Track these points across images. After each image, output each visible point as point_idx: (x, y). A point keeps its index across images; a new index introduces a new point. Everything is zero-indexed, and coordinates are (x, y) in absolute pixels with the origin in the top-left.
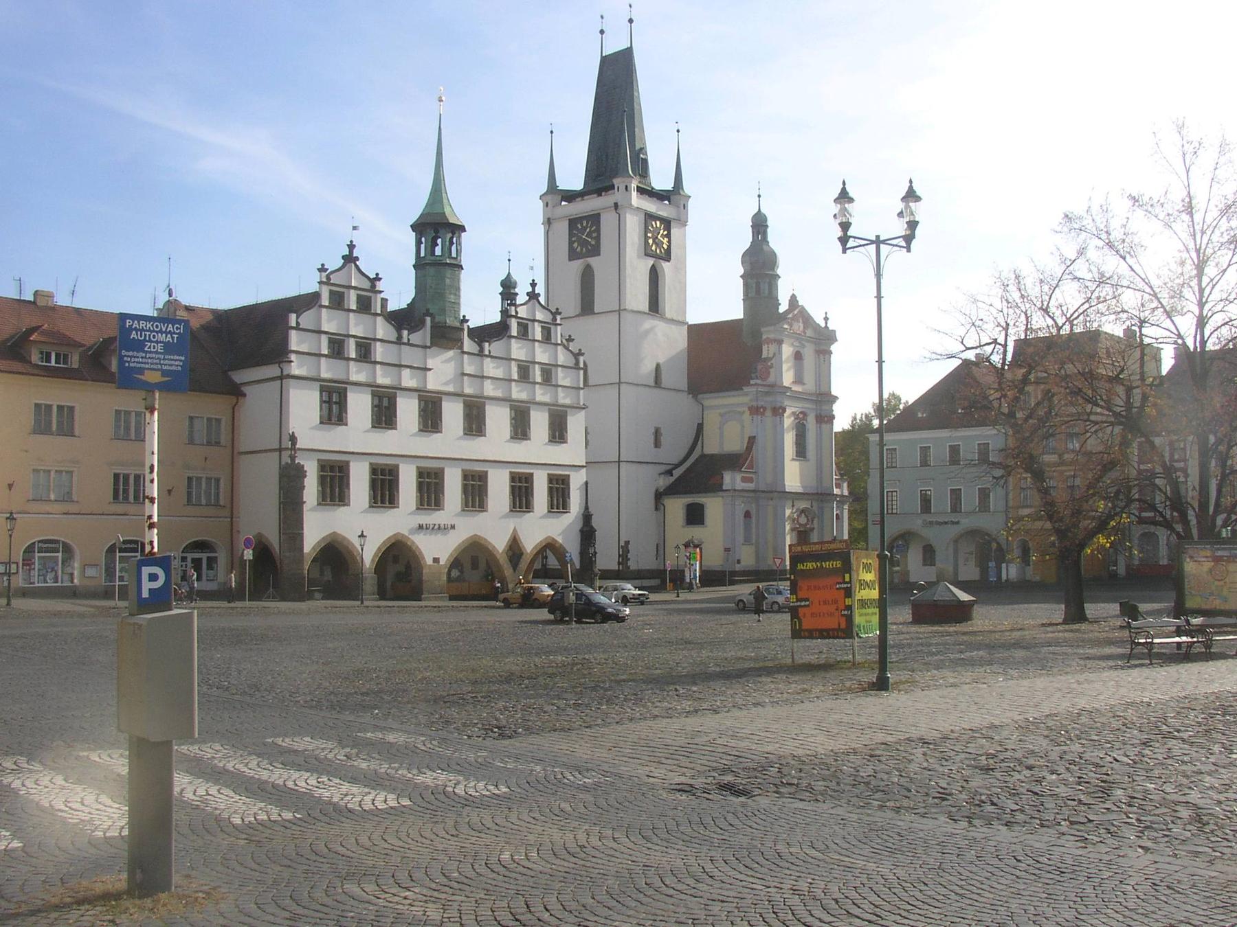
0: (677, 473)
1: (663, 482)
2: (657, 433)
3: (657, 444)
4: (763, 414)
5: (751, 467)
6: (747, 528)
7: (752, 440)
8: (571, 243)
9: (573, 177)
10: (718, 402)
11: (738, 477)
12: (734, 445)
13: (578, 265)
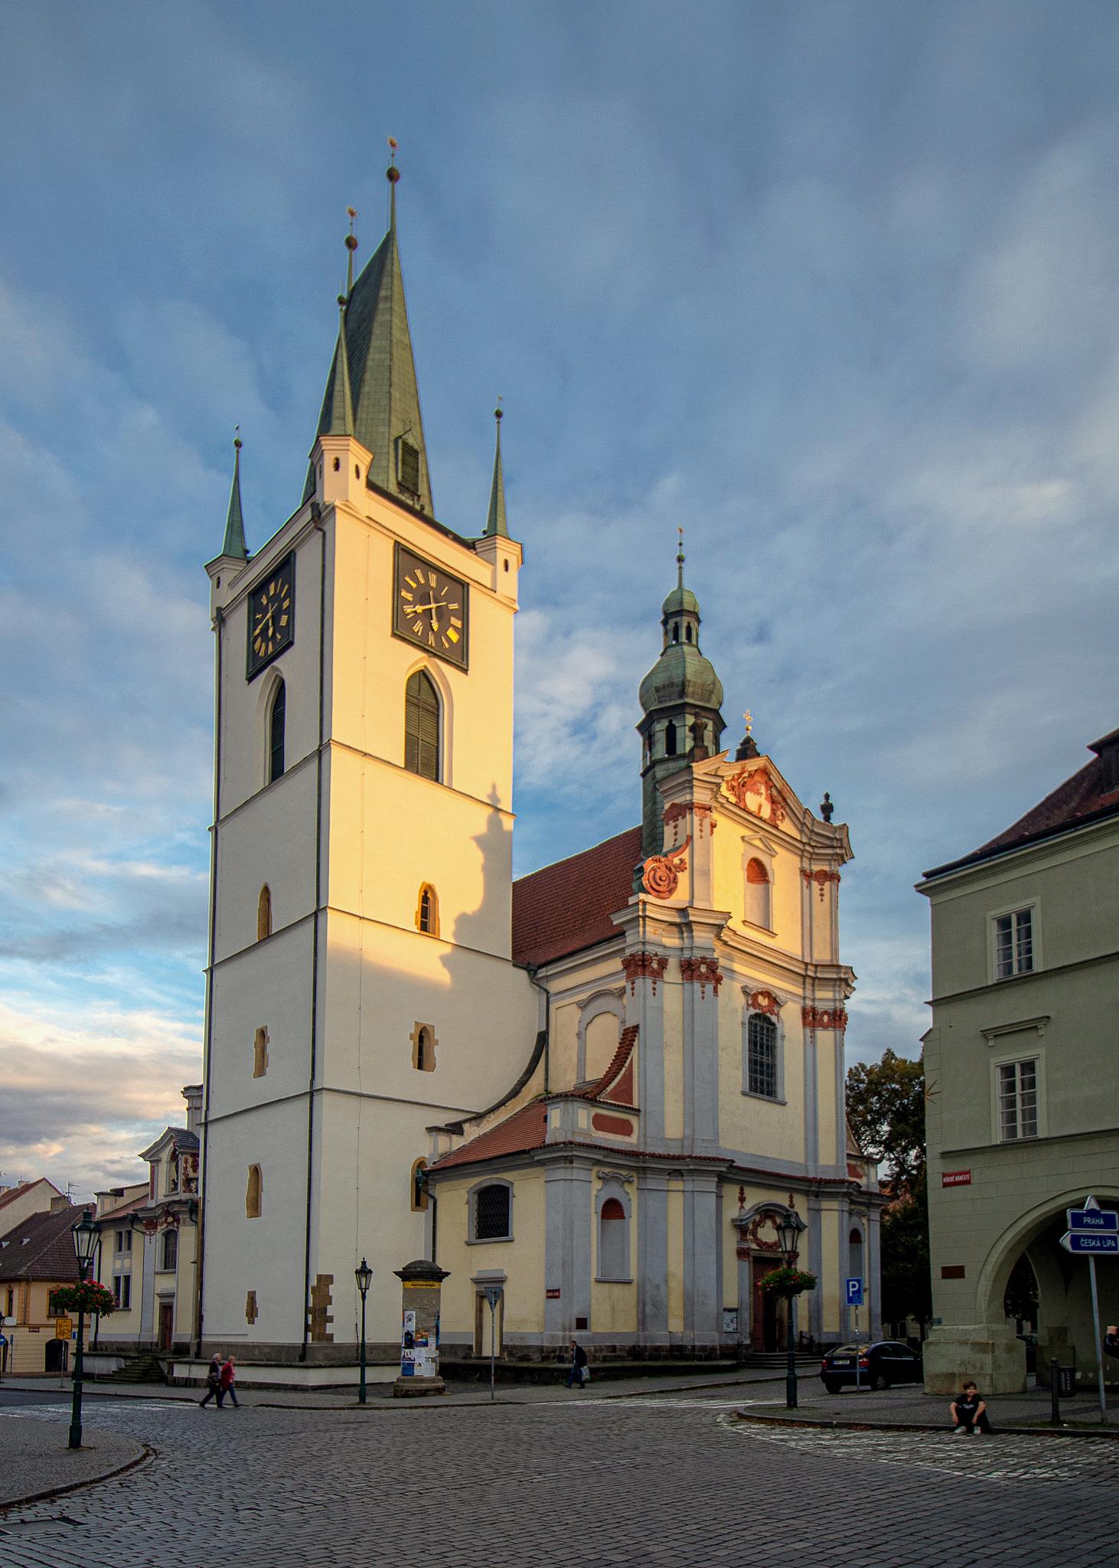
0: (472, 1132)
1: (433, 1149)
2: (423, 1039)
4: (658, 975)
5: (625, 1091)
7: (629, 1036)
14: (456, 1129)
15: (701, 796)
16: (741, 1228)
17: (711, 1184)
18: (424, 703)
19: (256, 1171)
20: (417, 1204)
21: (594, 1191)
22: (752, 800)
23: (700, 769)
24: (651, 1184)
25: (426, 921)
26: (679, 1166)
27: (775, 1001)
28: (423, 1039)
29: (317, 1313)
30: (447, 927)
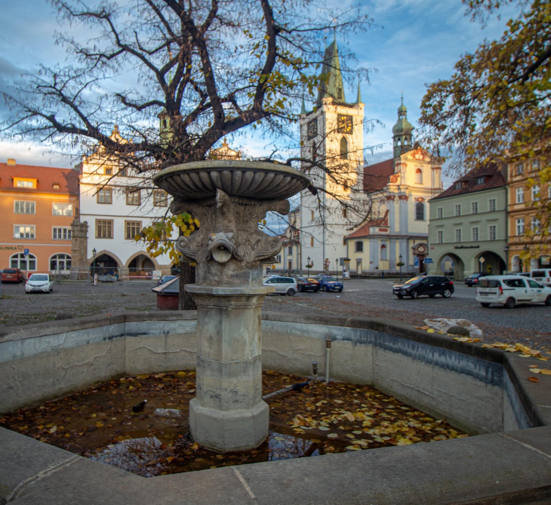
0: (355, 229)
1: (347, 233)
4: (393, 200)
14: (352, 229)
15: (402, 161)
16: (414, 249)
17: (405, 241)
21: (380, 243)
22: (417, 156)
23: (402, 156)
24: (392, 241)
26: (397, 237)
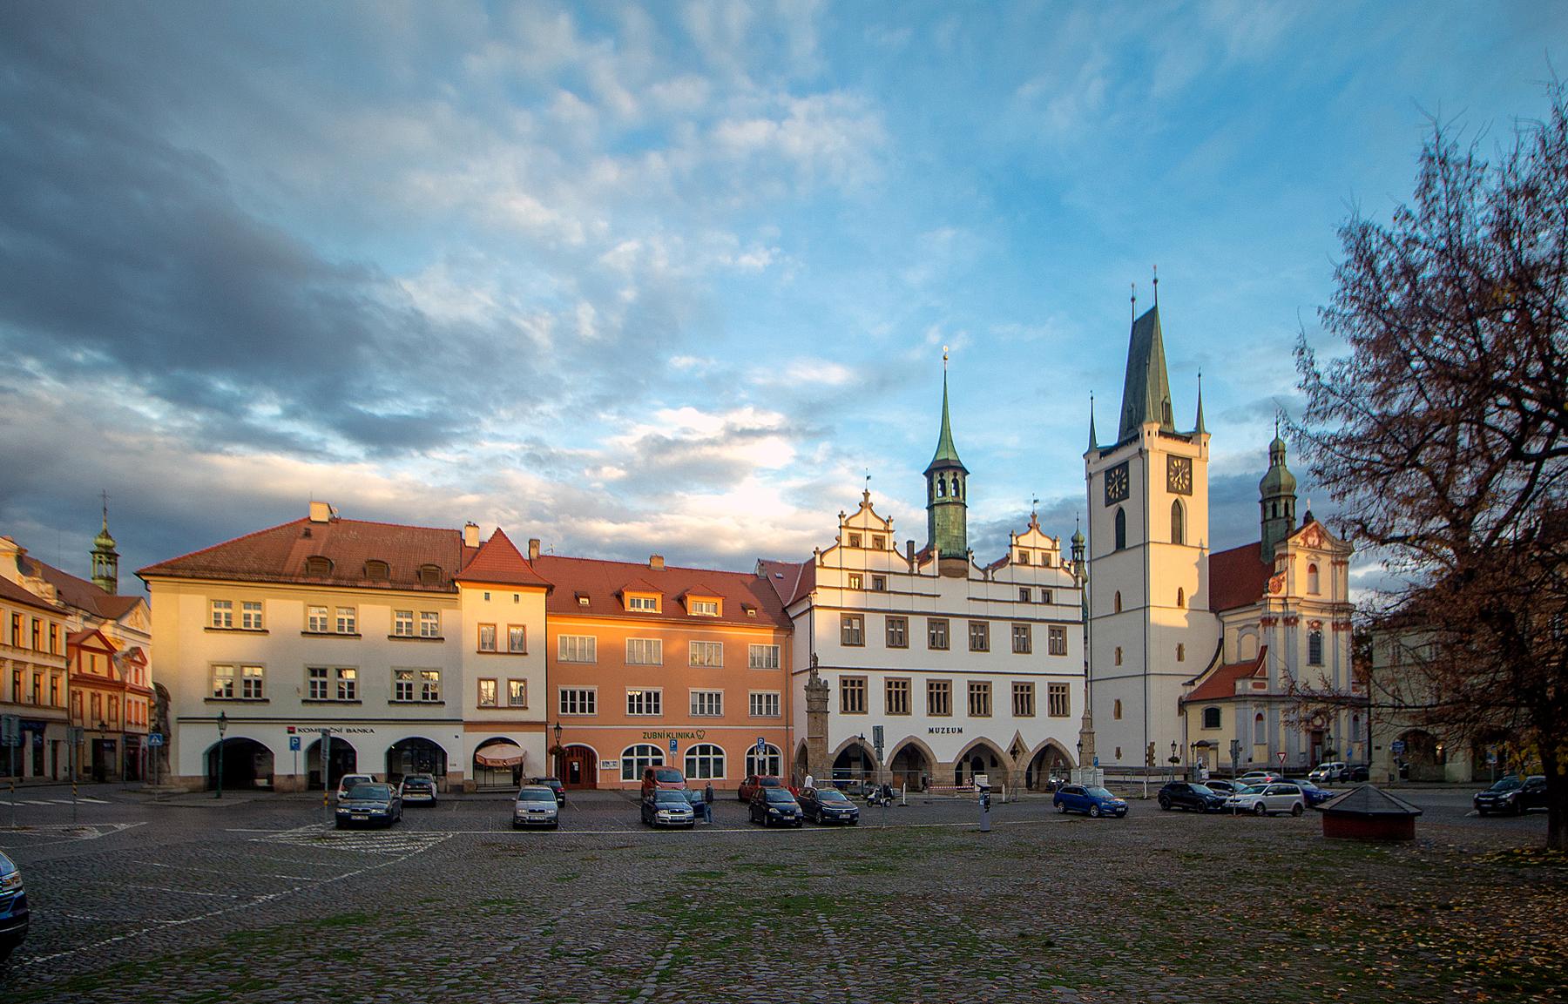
2: (1180, 648)
3: (1180, 658)
6: (1260, 732)
8: (1107, 491)
9: (1109, 435)
10: (1235, 618)
11: (1249, 684)
12: (1250, 654)
13: (1113, 508)
18: (1177, 511)
19: (1118, 702)
20: (1180, 713)
25: (1180, 603)
27: (1320, 623)
28: (1180, 648)
29: (1150, 756)
30: (1186, 604)
